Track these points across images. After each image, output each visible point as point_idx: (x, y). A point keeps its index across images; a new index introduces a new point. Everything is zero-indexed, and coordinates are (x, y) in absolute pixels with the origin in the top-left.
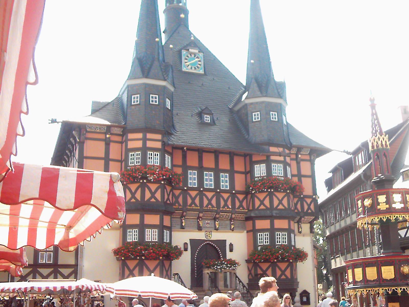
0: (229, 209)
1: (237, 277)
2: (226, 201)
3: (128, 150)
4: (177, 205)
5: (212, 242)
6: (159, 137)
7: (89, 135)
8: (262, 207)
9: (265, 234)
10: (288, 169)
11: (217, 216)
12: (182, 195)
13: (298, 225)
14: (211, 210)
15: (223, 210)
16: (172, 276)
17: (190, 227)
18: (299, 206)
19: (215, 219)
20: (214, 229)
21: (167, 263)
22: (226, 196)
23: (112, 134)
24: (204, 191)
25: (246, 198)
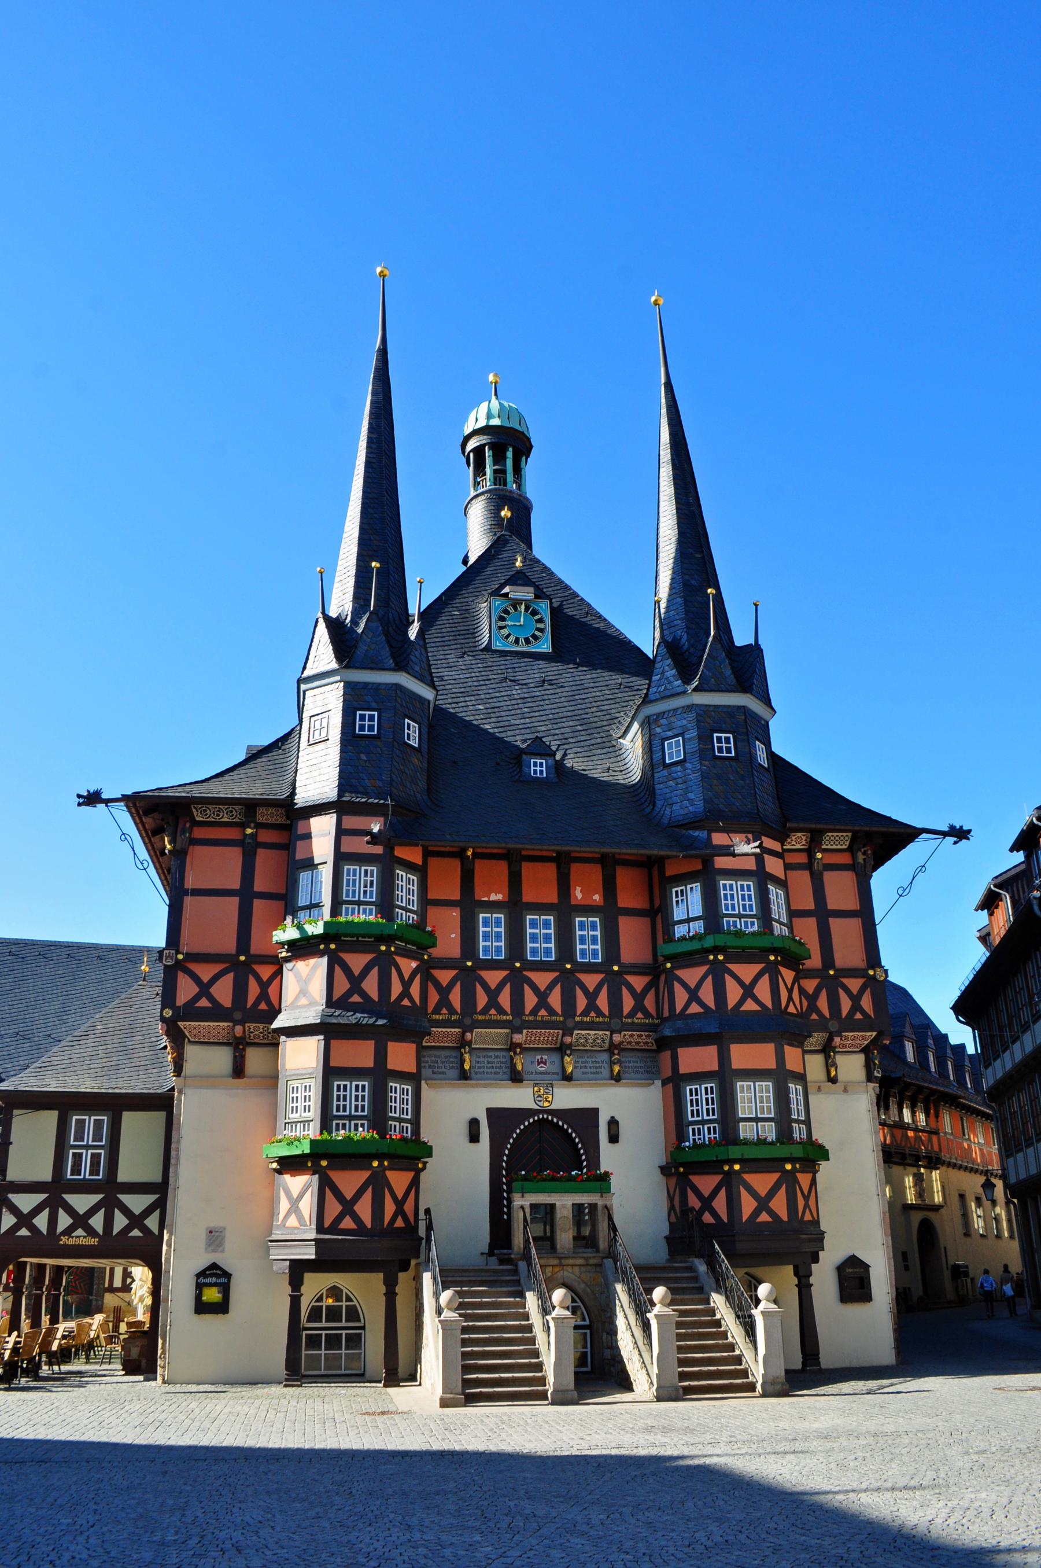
0: (601, 1019)
1: (610, 1218)
2: (592, 997)
4: (444, 1011)
5: (553, 1116)
7: (199, 833)
8: (695, 1008)
9: (706, 1088)
10: (776, 894)
11: (568, 1039)
12: (459, 984)
13: (827, 1058)
14: (547, 1022)
15: (582, 1022)
16: (422, 1215)
17: (488, 1073)
19: (562, 1050)
20: (560, 1076)
21: (399, 1180)
22: (591, 980)
23: (259, 826)
24: (526, 970)
25: (653, 984)
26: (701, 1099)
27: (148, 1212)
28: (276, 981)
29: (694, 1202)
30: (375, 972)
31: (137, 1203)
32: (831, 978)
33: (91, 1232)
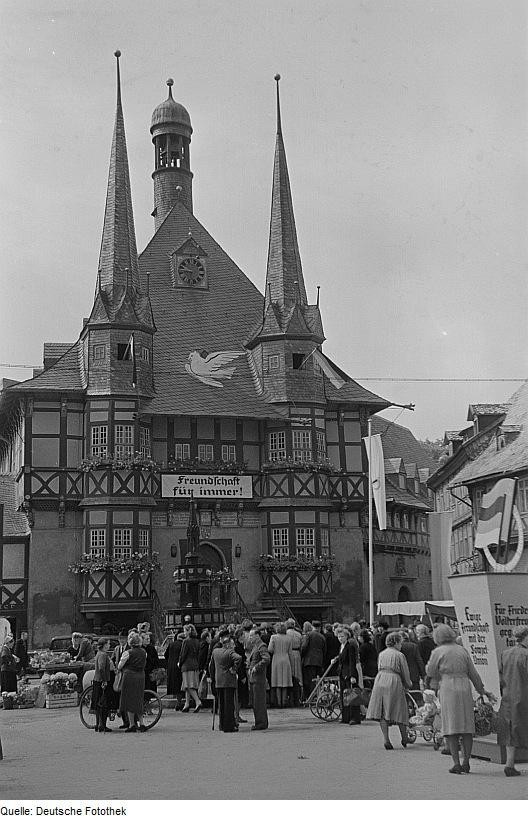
6: (132, 405)
18: (339, 489)
26: (280, 539)
27: (18, 593)
29: (276, 584)
31: (13, 588)
32: (344, 476)
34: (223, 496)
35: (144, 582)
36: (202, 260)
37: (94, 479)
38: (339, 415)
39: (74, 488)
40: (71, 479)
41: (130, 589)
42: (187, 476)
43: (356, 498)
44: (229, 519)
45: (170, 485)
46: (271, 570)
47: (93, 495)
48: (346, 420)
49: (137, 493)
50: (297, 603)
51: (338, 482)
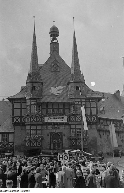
3: (27, 105)
6: (35, 101)
18: (90, 119)
28: (25, 119)
30: (36, 118)
33: (6, 147)
34: (60, 121)
35: (28, 143)
36: (58, 64)
37: (27, 118)
38: (90, 101)
39: (24, 120)
40: (23, 118)
41: (35, 144)
42: (51, 117)
43: (94, 121)
44: (62, 127)
45: (47, 119)
46: (70, 139)
47: (27, 122)
48: (91, 102)
49: (31, 122)
50: (77, 148)
51: (89, 117)
